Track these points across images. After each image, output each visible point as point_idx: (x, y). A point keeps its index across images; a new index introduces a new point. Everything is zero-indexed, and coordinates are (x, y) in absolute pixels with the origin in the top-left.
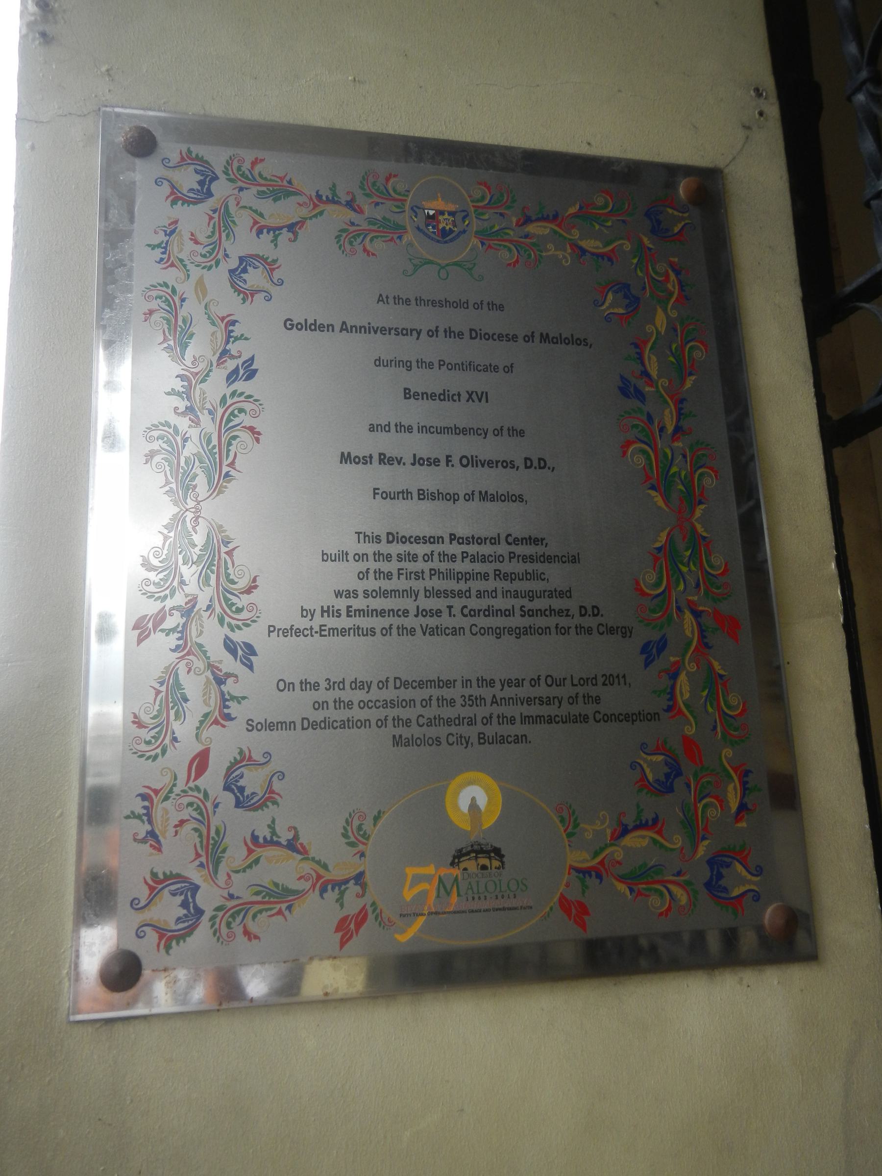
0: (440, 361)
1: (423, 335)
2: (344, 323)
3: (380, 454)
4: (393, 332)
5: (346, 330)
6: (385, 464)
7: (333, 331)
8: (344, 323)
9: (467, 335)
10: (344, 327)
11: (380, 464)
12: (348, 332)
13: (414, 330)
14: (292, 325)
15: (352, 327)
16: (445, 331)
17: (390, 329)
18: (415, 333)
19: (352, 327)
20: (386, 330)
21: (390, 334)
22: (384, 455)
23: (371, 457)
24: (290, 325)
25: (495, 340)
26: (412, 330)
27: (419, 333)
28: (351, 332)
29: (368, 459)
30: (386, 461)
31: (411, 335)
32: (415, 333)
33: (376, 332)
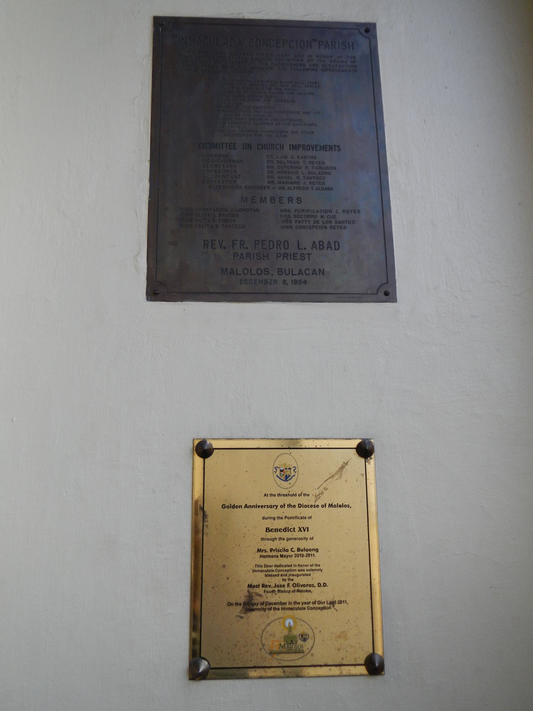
0: (285, 516)
1: (279, 507)
2: (246, 505)
3: (262, 584)
4: (266, 507)
5: (247, 507)
6: (264, 587)
7: (241, 508)
8: (246, 505)
9: (297, 506)
10: (246, 506)
11: (262, 587)
12: (248, 508)
13: (275, 505)
14: (225, 507)
15: (249, 506)
16: (288, 505)
17: (265, 506)
18: (275, 507)
19: (249, 506)
20: (263, 506)
21: (265, 507)
22: (264, 585)
23: (259, 585)
24: (224, 506)
25: (309, 507)
26: (274, 506)
27: (277, 506)
28: (249, 508)
29: (258, 586)
30: (265, 586)
31: (274, 507)
32: (275, 507)
33: (259, 507)
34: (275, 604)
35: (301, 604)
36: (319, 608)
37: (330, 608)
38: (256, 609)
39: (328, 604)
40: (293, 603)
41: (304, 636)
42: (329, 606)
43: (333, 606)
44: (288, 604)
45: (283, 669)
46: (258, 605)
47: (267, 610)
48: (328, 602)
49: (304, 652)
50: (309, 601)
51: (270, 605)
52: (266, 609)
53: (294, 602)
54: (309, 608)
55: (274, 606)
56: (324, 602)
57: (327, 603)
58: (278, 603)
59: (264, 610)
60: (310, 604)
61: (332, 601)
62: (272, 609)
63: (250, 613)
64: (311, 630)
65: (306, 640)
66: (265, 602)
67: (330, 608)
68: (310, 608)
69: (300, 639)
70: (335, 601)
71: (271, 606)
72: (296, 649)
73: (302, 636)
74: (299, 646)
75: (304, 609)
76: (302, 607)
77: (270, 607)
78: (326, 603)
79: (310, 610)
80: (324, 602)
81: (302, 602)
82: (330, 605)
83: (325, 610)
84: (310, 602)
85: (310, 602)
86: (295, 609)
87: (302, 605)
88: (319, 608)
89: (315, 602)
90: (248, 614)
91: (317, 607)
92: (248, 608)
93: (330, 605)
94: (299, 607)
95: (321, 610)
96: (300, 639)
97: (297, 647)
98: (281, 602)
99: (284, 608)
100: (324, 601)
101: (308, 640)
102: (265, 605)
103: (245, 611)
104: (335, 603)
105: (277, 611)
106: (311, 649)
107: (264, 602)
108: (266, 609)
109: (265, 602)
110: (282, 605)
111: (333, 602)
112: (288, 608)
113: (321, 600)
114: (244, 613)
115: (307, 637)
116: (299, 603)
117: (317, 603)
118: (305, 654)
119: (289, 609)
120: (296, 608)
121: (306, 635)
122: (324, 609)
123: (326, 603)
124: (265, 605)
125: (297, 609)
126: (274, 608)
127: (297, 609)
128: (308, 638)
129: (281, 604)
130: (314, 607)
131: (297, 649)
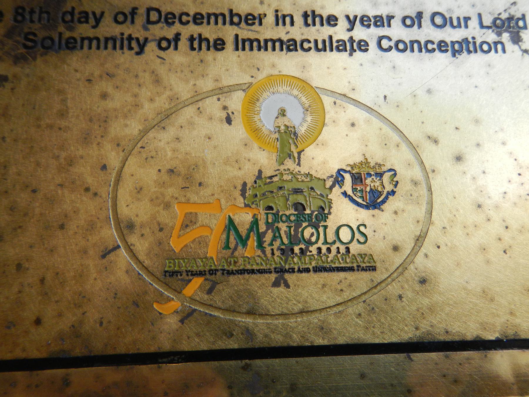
34: (198, 19)
35: (343, 24)
36: (442, 46)
37: (499, 47)
38: (90, 40)
39: (488, 27)
40: (299, 20)
41: (368, 181)
42: (491, 37)
43: (516, 39)
44: (270, 19)
45: (245, 368)
46: (98, 21)
47: (151, 47)
48: (487, 21)
49: (374, 269)
50: (383, 11)
51: (170, 24)
52: (146, 40)
53: (305, 15)
54: (385, 43)
55: (193, 29)
56: (467, 19)
57: (482, 26)
58: (216, 16)
59: (134, 44)
60: (389, 25)
61: (504, 16)
62: (183, 44)
63: (52, 58)
64: (406, 153)
65: (384, 202)
66: (142, 11)
67: (499, 47)
68: (392, 44)
69: (345, 194)
70: (519, 15)
71: (177, 27)
72: (324, 250)
73: (357, 179)
74: (345, 235)
75: (363, 46)
76: (351, 39)
77: (170, 33)
78: (474, 23)
79: (394, 50)
80: (467, 19)
81: (348, 17)
82: (499, 34)
83: (473, 55)
84: (390, 18)
85: (390, 18)
86: (312, 45)
87: (350, 30)
88: (442, 46)
89: (420, 15)
90: (39, 61)
91: (433, 43)
92: (41, 34)
93: (499, 34)
94: (331, 37)
95: (454, 55)
96: (345, 194)
97: (331, 237)
98: (231, 11)
99: (251, 41)
100: (467, 15)
101: (392, 204)
102: (140, 20)
103: (22, 50)
104: (521, 23)
105: (210, 56)
106: (414, 252)
107: (134, 11)
108: (146, 40)
109: (142, 11)
110: (238, 24)
111: (510, 18)
112: (274, 41)
113: (449, 10)
114: (18, 60)
115: (389, 188)
116: (332, 20)
117: (426, 21)
118: (379, 276)
119: (277, 44)
120: (316, 41)
121: (380, 175)
122: (469, 52)
123: (474, 23)
124: (140, 20)
125: (320, 46)
126: (192, 39)
127: (320, 46)
128: (393, 193)
129: (232, 23)
130: (412, 42)
131: (334, 249)
